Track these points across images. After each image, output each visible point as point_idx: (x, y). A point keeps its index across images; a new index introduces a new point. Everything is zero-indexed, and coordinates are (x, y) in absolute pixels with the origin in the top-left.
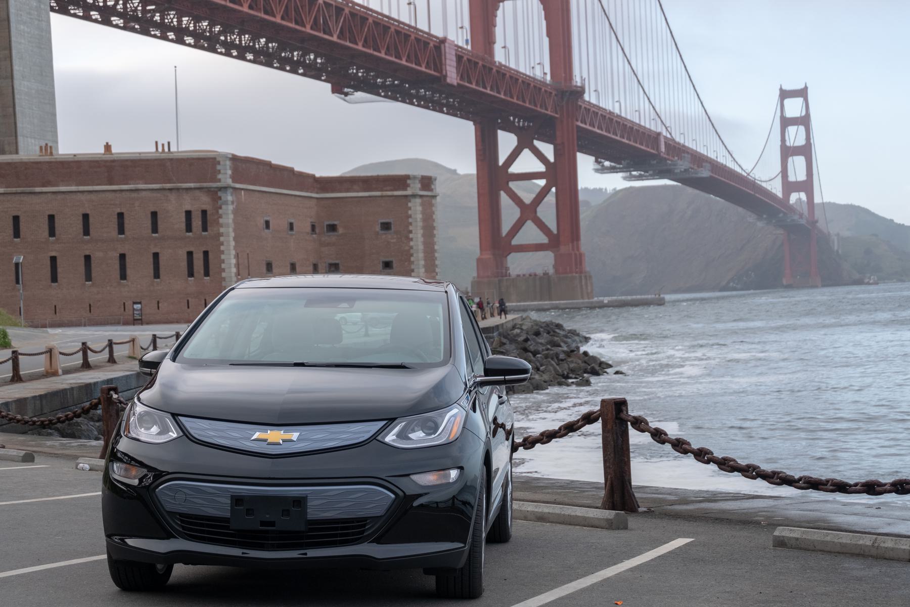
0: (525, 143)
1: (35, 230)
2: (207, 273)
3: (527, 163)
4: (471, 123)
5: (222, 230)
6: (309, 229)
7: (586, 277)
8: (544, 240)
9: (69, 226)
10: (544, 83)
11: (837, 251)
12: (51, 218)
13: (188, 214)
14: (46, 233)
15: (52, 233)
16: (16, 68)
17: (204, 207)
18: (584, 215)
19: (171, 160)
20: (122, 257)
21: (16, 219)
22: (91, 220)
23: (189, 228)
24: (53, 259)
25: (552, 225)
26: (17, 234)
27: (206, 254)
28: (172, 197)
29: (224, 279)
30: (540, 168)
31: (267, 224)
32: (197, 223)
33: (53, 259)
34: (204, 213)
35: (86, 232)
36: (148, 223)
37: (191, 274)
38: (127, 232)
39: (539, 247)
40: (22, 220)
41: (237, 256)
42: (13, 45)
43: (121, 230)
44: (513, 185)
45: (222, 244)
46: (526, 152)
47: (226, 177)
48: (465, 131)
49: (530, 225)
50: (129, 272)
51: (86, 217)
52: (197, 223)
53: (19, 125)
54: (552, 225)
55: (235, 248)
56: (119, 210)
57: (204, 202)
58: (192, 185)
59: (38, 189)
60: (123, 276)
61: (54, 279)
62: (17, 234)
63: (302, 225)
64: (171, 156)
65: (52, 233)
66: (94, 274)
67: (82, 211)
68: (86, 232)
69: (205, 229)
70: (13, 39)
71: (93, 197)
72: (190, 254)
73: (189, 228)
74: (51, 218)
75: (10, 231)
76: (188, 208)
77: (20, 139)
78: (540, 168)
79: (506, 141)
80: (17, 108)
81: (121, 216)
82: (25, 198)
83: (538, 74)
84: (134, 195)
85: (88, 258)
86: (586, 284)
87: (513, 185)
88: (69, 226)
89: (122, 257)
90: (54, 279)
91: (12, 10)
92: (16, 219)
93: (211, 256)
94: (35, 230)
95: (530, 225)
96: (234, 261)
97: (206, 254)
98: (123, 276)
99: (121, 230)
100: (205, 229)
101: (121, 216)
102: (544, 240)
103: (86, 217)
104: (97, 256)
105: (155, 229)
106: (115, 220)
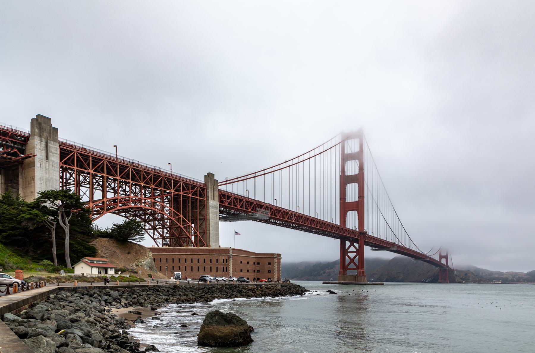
0: (352, 244)
1: (195, 261)
2: (226, 271)
3: (352, 249)
4: (339, 240)
5: (230, 263)
6: (253, 263)
7: (365, 277)
8: (355, 267)
9: (201, 261)
10: (356, 231)
11: (456, 274)
12: (198, 259)
13: (224, 260)
14: (197, 262)
15: (198, 262)
16: (211, 228)
17: (227, 258)
18: (365, 262)
19: (221, 249)
20: (211, 267)
21: (192, 259)
22: (205, 260)
23: (223, 262)
24: (198, 267)
25: (357, 264)
26: (192, 262)
27: (226, 267)
28: (221, 256)
29: (230, 272)
30: (355, 250)
31: (241, 262)
32: (225, 261)
33: (198, 267)
34: (226, 260)
35: (204, 262)
36: (216, 261)
37: (223, 271)
38: (212, 263)
39: (354, 269)
40: (193, 259)
41: (233, 268)
42: (210, 224)
43: (211, 262)
44: (348, 254)
45: (230, 266)
46: (352, 246)
47: (231, 253)
48: (338, 241)
49: (352, 264)
50: (212, 270)
51: (204, 259)
52: (225, 261)
53: (210, 240)
54: (357, 264)
55: (232, 267)
56: (210, 258)
57: (226, 257)
58: (224, 254)
59: (196, 254)
60: (211, 271)
61: (198, 271)
62: (192, 262)
63: (251, 263)
64: (220, 248)
65: (198, 262)
66: (205, 270)
67: (204, 258)
68: (204, 262)
69: (226, 263)
70: (210, 223)
71: (206, 256)
72: (223, 267)
73: (223, 262)
74: (198, 259)
75: (191, 261)
76: (224, 258)
77: (211, 243)
78: (355, 250)
79: (348, 244)
80: (210, 237)
81: (211, 259)
82: (194, 255)
83: (354, 229)
84: (214, 256)
85: (204, 267)
86: (365, 278)
87: (348, 254)
88: (201, 261)
89: (211, 267)
90: (198, 271)
91: (210, 217)
92: (192, 259)
93: (227, 268)
94: (195, 261)
95: (352, 264)
96: (232, 269)
97: (226, 267)
98: (211, 271)
99: (211, 262)
100: (226, 263)
101: (211, 259)
102: (355, 267)
103: (204, 259)
104: (206, 267)
105: (217, 262)
106: (210, 260)
